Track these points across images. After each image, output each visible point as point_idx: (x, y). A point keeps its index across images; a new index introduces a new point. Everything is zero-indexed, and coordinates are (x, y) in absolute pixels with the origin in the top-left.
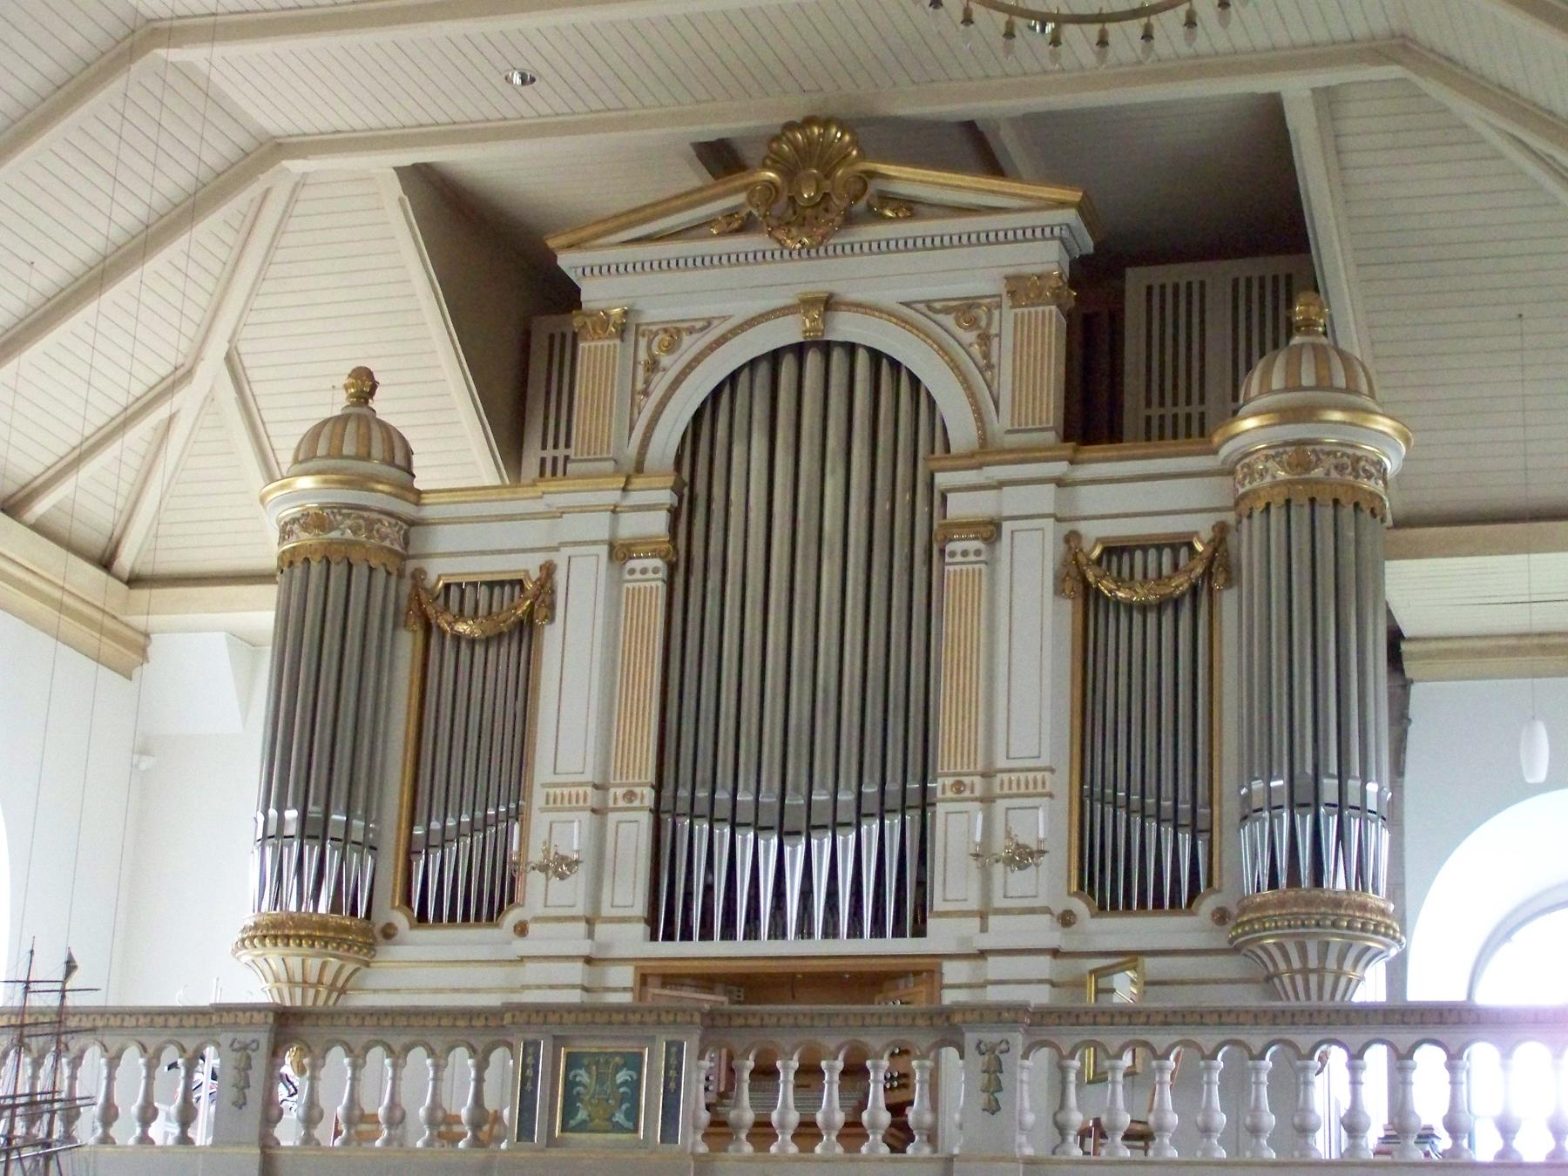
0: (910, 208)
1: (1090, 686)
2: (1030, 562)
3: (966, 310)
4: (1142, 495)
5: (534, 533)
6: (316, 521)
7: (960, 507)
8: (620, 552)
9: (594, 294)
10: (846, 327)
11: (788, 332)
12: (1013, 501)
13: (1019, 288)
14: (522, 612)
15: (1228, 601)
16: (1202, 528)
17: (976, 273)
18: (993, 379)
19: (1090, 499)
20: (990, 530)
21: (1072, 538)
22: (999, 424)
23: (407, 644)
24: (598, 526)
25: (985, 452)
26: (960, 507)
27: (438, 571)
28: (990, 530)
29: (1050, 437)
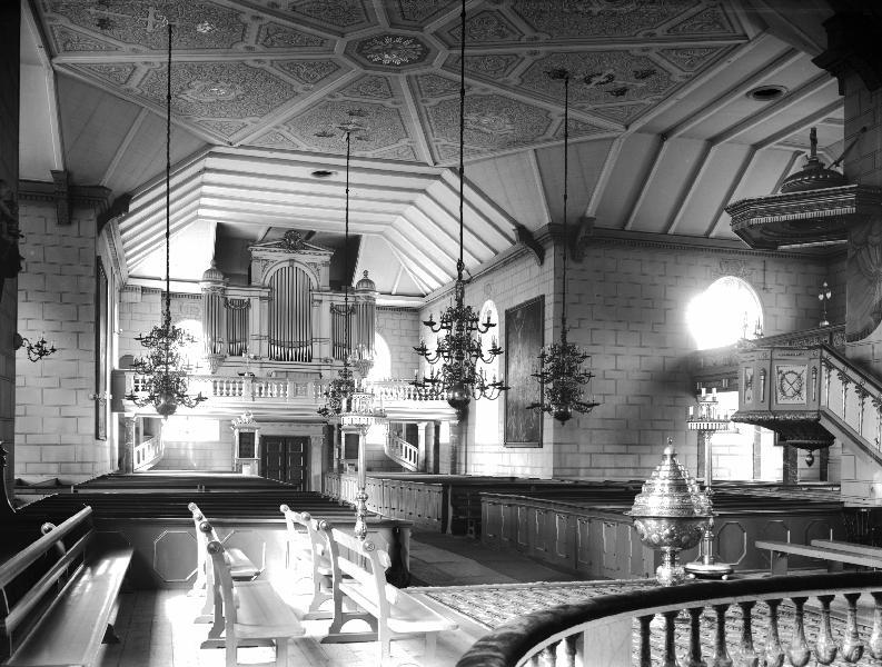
0: (308, 248)
1: (146, 251)
2: (326, 307)
4: (339, 299)
5: (247, 293)
6: (214, 289)
8: (261, 298)
12: (324, 298)
13: (325, 264)
14: (244, 306)
15: (354, 317)
18: (322, 278)
19: (334, 298)
20: (321, 301)
21: (332, 304)
22: (321, 284)
24: (257, 294)
26: (316, 297)
27: (229, 298)
28: (321, 301)
29: (329, 288)
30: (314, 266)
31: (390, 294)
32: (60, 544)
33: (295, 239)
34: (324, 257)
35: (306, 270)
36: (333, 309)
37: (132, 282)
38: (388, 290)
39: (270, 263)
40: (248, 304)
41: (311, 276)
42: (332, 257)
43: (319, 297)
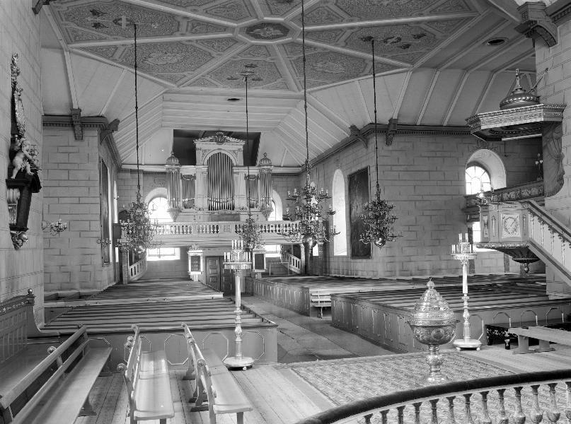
0: (228, 141)
2: (242, 176)
3: (234, 151)
4: (254, 171)
7: (235, 171)
9: (198, 146)
10: (223, 152)
11: (216, 152)
12: (240, 171)
14: (190, 180)
16: (256, 174)
17: (235, 148)
18: (238, 159)
23: (181, 181)
25: (237, 166)
28: (238, 173)
30: (233, 149)
31: (280, 167)
32: (60, 360)
33: (220, 135)
34: (239, 145)
35: (229, 155)
36: (248, 178)
37: (124, 167)
38: (279, 165)
39: (205, 148)
40: (195, 177)
41: (232, 158)
42: (244, 146)
43: (238, 171)
